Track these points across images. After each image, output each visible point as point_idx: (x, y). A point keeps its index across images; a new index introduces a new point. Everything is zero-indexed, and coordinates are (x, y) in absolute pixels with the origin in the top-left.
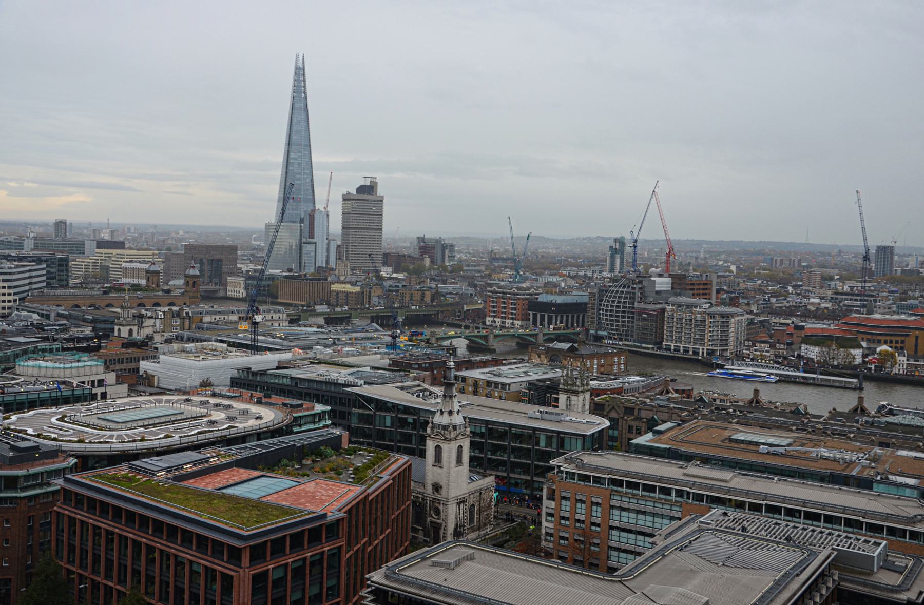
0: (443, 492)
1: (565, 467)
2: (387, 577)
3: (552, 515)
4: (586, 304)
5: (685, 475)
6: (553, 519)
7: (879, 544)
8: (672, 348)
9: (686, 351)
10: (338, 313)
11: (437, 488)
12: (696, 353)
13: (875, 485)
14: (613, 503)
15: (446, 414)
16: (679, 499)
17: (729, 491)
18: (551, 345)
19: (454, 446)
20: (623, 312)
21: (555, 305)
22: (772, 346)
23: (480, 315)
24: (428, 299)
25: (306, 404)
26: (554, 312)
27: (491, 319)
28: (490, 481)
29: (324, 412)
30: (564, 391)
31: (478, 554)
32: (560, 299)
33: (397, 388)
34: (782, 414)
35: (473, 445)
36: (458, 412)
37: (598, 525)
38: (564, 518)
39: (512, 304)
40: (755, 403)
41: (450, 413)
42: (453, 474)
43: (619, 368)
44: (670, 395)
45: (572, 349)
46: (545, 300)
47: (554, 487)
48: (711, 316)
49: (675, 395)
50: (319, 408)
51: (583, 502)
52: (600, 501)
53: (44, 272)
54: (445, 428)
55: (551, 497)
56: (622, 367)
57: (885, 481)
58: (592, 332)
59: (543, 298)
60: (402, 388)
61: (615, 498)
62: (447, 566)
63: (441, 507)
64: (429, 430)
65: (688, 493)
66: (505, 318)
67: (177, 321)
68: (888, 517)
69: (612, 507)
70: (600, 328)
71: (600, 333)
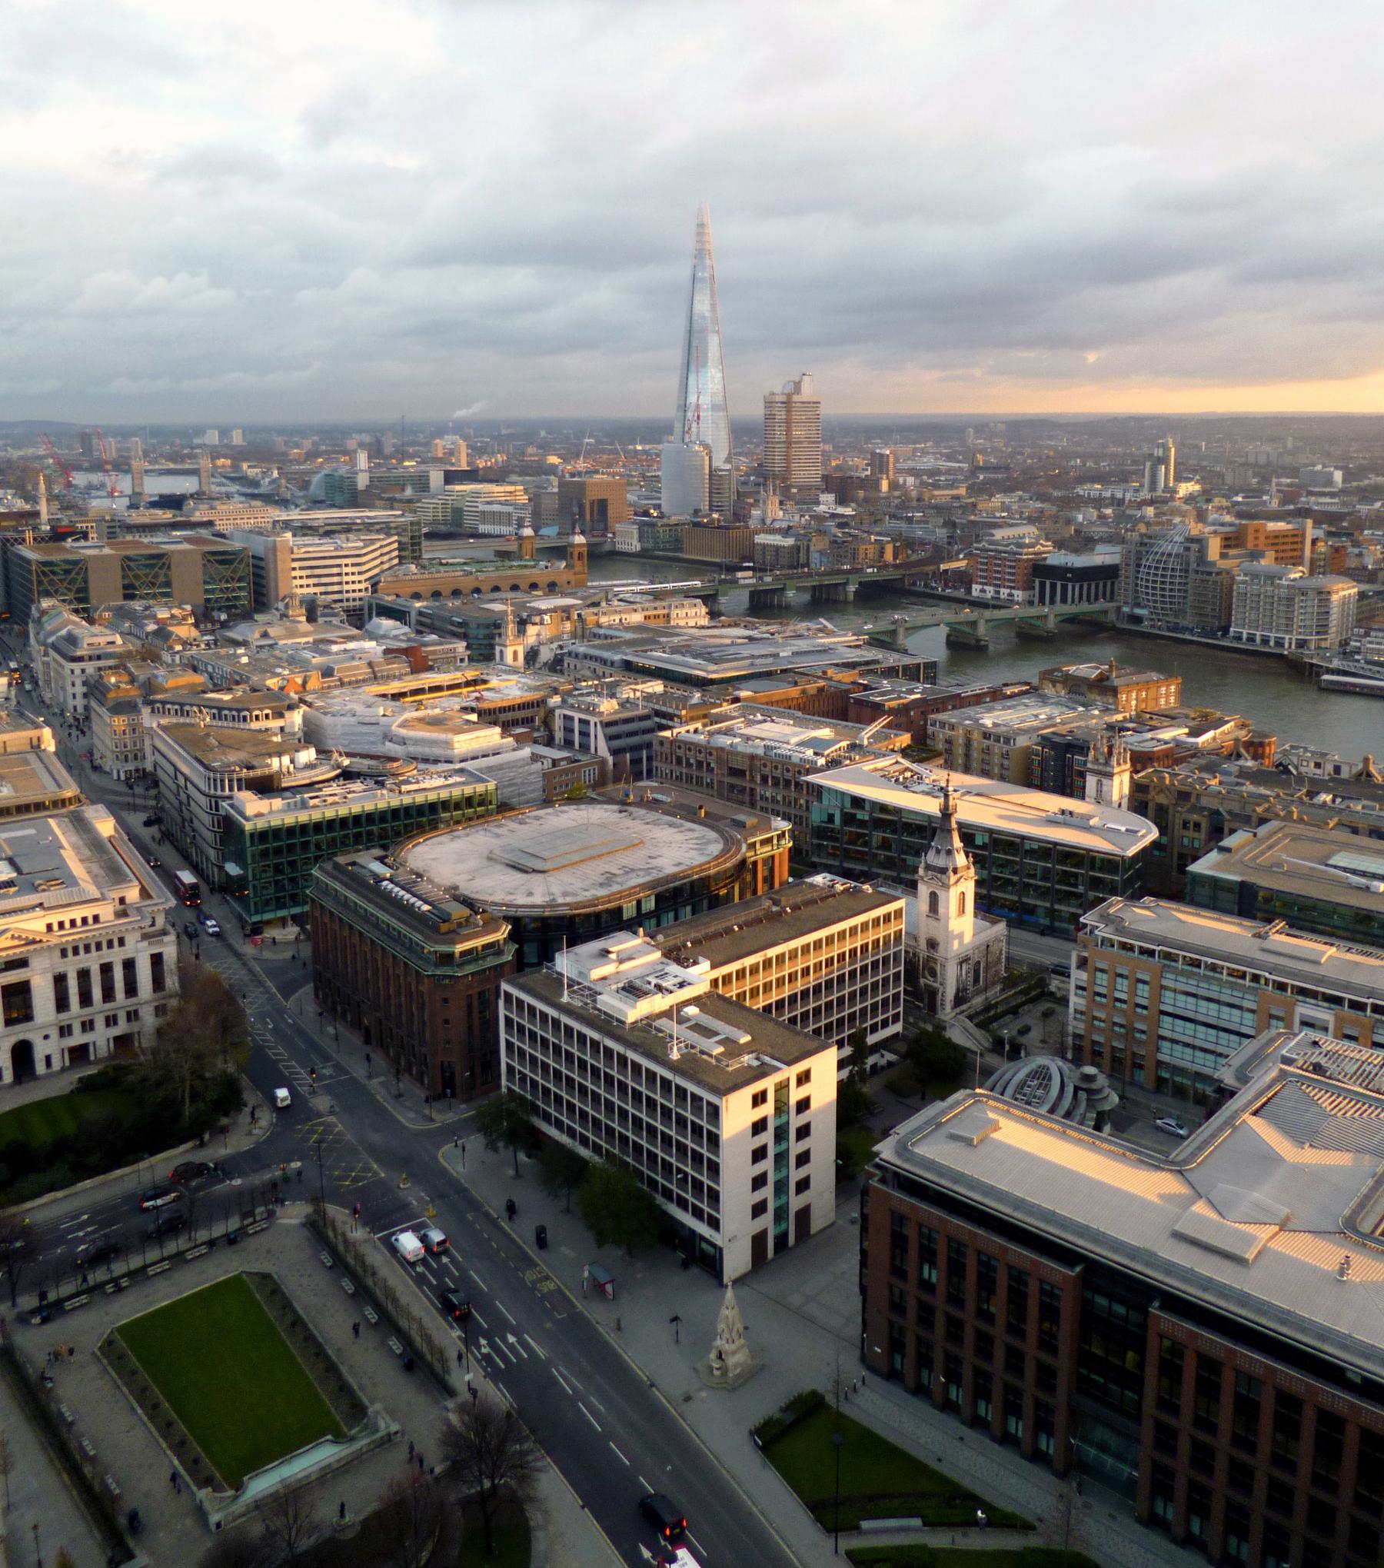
0: (941, 949)
2: (898, 1154)
3: (1083, 989)
8: (1245, 636)
9: (1265, 641)
10: (768, 584)
11: (932, 944)
12: (1279, 643)
14: (1165, 982)
15: (943, 854)
20: (1171, 583)
24: (889, 556)
26: (1069, 580)
27: (979, 587)
32: (1079, 561)
37: (1145, 1008)
39: (1011, 567)
47: (1086, 954)
48: (1304, 593)
54: (943, 871)
55: (1083, 963)
58: (1126, 609)
61: (1169, 975)
64: (921, 872)
65: (1267, 980)
66: (999, 586)
69: (1163, 987)
70: (1138, 605)
71: (1138, 611)
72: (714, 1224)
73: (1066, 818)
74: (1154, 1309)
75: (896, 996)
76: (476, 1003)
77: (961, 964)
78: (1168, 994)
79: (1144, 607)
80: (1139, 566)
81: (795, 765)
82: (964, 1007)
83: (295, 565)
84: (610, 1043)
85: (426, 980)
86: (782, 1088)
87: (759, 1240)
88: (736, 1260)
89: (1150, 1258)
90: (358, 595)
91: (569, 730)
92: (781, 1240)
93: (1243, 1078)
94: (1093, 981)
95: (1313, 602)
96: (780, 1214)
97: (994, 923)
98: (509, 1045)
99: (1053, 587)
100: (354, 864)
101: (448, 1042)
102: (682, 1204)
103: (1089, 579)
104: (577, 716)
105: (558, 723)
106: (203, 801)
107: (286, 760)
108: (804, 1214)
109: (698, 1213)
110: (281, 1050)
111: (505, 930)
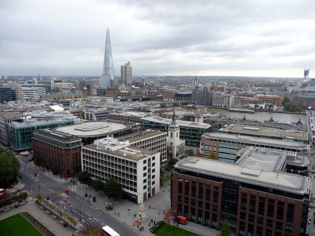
0: (173, 144)
1: (206, 137)
2: (179, 166)
3: (203, 150)
4: (191, 94)
5: (238, 138)
6: (203, 150)
7: (295, 153)
10: (124, 98)
11: (171, 144)
12: (221, 106)
13: (283, 139)
15: (173, 124)
16: (237, 144)
17: (250, 141)
18: (187, 105)
19: (176, 132)
20: (201, 96)
21: (182, 95)
22: (242, 104)
23: (161, 98)
24: (147, 94)
25: (134, 123)
26: (182, 96)
27: (165, 99)
28: (184, 141)
29: (139, 125)
30: (196, 117)
31: (200, 160)
33: (154, 118)
34: (252, 122)
35: (180, 133)
36: (177, 124)
37: (215, 152)
38: (206, 150)
40: (244, 119)
41: (175, 124)
42: (176, 140)
43: (206, 111)
44: (222, 118)
45: (193, 106)
46: (179, 93)
47: (203, 142)
48: (225, 97)
49: (224, 118)
50: (137, 124)
51: (211, 146)
52: (216, 145)
53: (45, 90)
54: (174, 128)
55: (202, 144)
56: (206, 111)
57: (285, 138)
58: (193, 101)
59: (179, 93)
60: (154, 118)
62: (194, 163)
63: (173, 149)
65: (240, 143)
67: (85, 102)
68: (292, 147)
70: (195, 101)
72: (135, 190)
73: (193, 124)
74: (240, 187)
75: (165, 153)
76: (75, 155)
77: (177, 147)
78: (220, 148)
79: (196, 101)
80: (195, 93)
81: (138, 118)
82: (178, 157)
83: (23, 92)
84: (109, 155)
85: (63, 150)
86: (149, 160)
87: (145, 194)
88: (140, 199)
89: (238, 177)
90: (37, 99)
91: (87, 116)
92: (149, 195)
93: (242, 154)
94: (204, 148)
95: (227, 98)
96: (149, 189)
97: (183, 140)
98: (84, 161)
99: (179, 98)
100: (43, 131)
101: (68, 165)
102: (127, 188)
103: (185, 96)
104: (89, 113)
105: (85, 115)
106: (3, 126)
107: (24, 118)
108: (154, 189)
109: (131, 189)
110: (26, 172)
111: (81, 140)
